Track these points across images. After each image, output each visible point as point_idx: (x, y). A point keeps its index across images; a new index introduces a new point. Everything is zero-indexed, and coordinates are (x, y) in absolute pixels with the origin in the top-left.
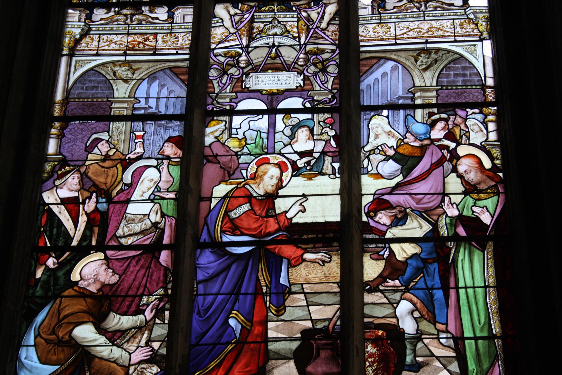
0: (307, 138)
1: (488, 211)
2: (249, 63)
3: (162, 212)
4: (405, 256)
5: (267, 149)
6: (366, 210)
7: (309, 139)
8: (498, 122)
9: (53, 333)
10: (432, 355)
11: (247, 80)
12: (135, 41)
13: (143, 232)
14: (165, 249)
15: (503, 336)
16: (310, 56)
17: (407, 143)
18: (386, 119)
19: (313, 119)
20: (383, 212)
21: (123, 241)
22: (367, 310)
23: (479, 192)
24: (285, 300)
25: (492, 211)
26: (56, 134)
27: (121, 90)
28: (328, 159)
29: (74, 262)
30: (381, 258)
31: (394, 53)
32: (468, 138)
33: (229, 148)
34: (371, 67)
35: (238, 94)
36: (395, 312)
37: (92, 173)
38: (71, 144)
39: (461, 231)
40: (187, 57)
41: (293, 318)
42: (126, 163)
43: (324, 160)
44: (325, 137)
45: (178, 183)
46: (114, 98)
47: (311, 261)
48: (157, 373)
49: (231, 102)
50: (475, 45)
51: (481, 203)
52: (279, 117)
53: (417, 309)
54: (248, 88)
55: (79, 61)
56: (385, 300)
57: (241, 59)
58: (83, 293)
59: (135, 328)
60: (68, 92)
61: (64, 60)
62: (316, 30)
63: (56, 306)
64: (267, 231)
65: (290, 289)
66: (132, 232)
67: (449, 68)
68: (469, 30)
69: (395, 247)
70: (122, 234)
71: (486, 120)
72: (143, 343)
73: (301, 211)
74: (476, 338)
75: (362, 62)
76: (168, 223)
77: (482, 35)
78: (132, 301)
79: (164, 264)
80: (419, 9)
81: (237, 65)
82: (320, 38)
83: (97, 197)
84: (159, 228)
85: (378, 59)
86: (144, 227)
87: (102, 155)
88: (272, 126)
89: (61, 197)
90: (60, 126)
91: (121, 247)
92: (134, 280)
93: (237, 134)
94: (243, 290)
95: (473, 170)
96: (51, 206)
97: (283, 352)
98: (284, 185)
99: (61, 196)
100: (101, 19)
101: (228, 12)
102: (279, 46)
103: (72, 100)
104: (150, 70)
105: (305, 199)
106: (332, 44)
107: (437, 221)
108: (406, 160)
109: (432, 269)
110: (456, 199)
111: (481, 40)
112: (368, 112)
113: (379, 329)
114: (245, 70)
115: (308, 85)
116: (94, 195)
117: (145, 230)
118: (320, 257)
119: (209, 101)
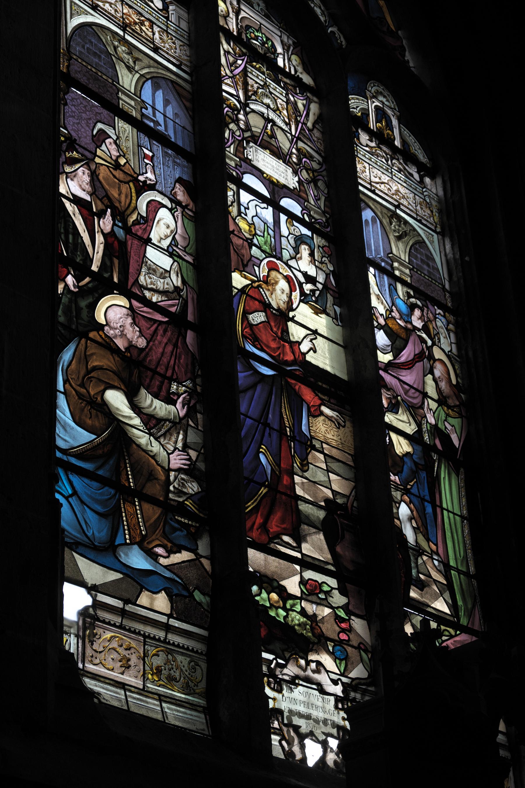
9: (82, 385)
31: (372, 201)
33: (241, 229)
58: (110, 345)
66: (154, 287)
72: (180, 445)
88: (277, 224)
92: (163, 354)
95: (444, 379)
98: (294, 306)
109: (423, 478)
118: (335, 416)
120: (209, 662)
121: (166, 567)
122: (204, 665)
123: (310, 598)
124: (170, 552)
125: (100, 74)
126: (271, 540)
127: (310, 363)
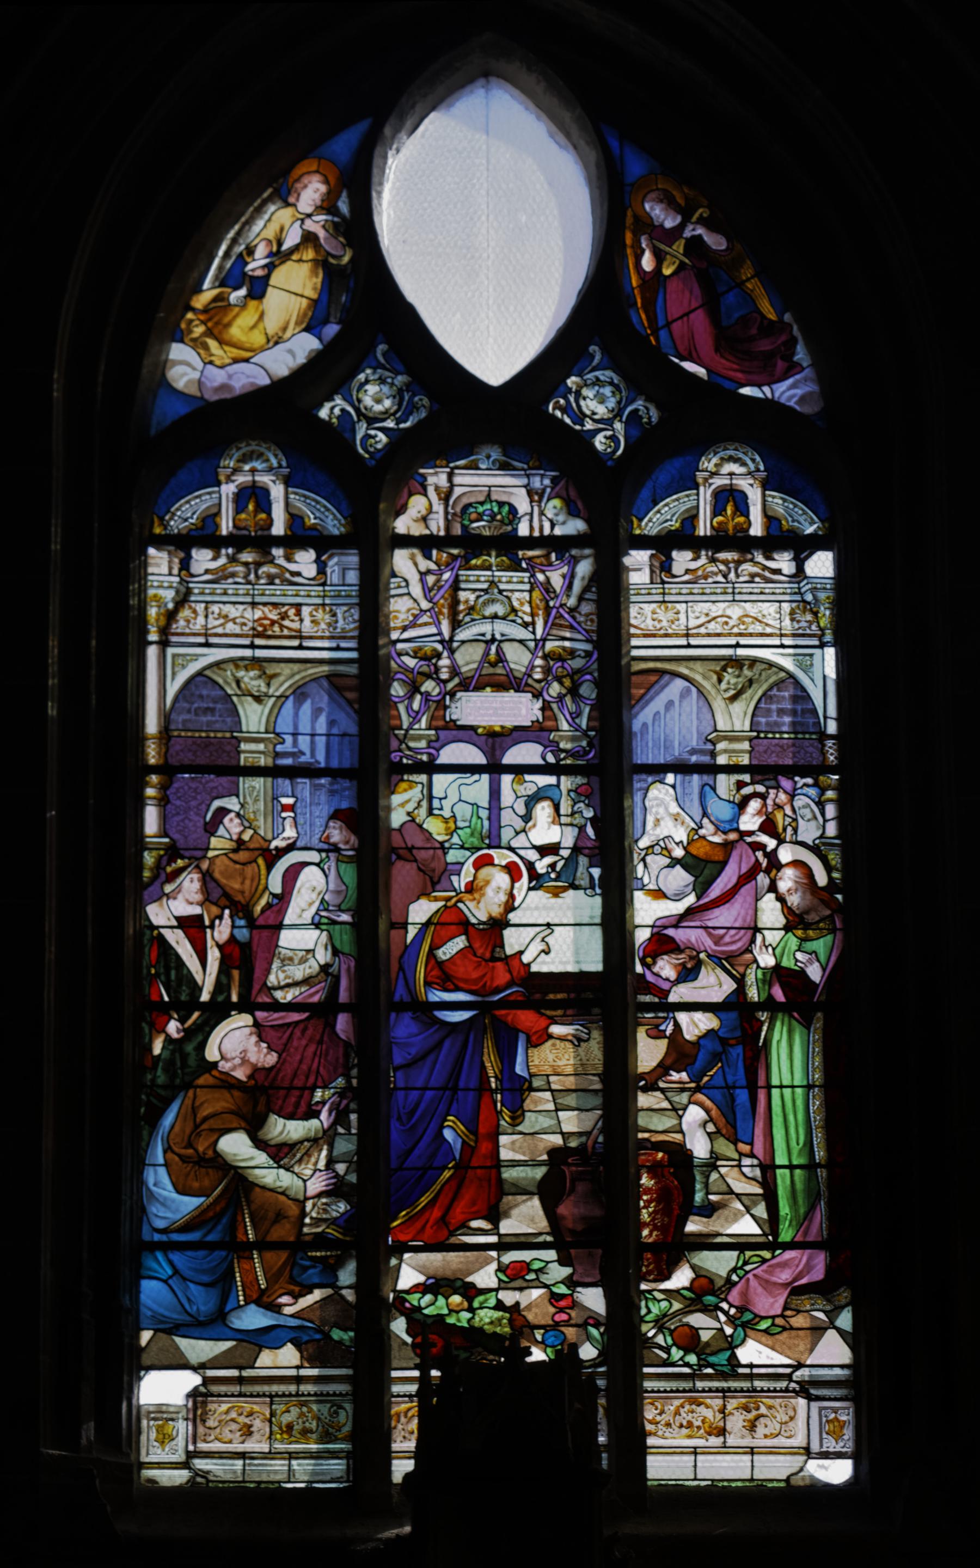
0: (550, 820)
1: (818, 961)
2: (454, 671)
3: (334, 947)
4: (697, 1032)
5: (489, 837)
6: (641, 954)
7: (553, 822)
8: (841, 803)
9: (190, 1145)
10: (731, 1192)
11: (453, 705)
12: (266, 618)
13: (306, 981)
14: (343, 1011)
15: (830, 1164)
16: (552, 663)
17: (704, 837)
18: (671, 791)
19: (558, 786)
20: (665, 957)
21: (279, 995)
22: (642, 1120)
23: (807, 926)
24: (523, 1101)
25: (823, 958)
26: (154, 798)
27: (253, 717)
28: (583, 861)
29: (208, 1029)
30: (659, 1035)
31: (684, 663)
32: (795, 830)
34: (648, 690)
35: (440, 732)
36: (680, 1124)
37: (221, 873)
38: (180, 817)
39: (778, 994)
40: (354, 655)
41: (537, 1129)
42: (272, 857)
43: (577, 863)
44: (578, 820)
45: (355, 895)
46: (241, 732)
47: (562, 1039)
48: (347, 1212)
49: (429, 747)
50: (811, 655)
51: (810, 946)
52: (507, 779)
53: (711, 1120)
54: (454, 721)
55: (179, 655)
56: (665, 1105)
57: (441, 663)
59: (308, 1140)
60: (166, 718)
61: (152, 652)
62: (561, 610)
63: (188, 1102)
64: (495, 985)
65: (530, 1083)
66: (290, 981)
67: (771, 697)
68: (804, 624)
69: (682, 1017)
70: (276, 983)
71: (823, 798)
72: (322, 1164)
73: (543, 951)
74: (791, 1167)
75: (634, 679)
76: (344, 967)
77: (823, 635)
78: (301, 1097)
79: (343, 1036)
80: (725, 576)
81: (433, 674)
82: (566, 627)
83: (231, 916)
84: (331, 974)
85: (660, 674)
86: (308, 971)
87: (231, 840)
89: (177, 914)
90: (159, 783)
91: (276, 1006)
92: (301, 1061)
93: (441, 809)
94: (462, 1084)
96: (162, 931)
97: (523, 1184)
98: (516, 904)
99: (177, 914)
100: (207, 571)
101: (416, 564)
102: (501, 641)
103: (176, 733)
104: (297, 677)
105: (549, 931)
106: (587, 641)
107: (743, 976)
108: (701, 865)
109: (735, 1055)
110: (773, 937)
111: (822, 646)
112: (644, 776)
113: (658, 1150)
114: (450, 686)
115: (549, 719)
116: (227, 912)
117: (311, 977)
119: (394, 744)
120: (355, 1402)
121: (292, 1316)
122: (348, 1406)
123: (512, 1285)
124: (296, 1297)
125: (212, 735)
126: (452, 1234)
127: (539, 974)
